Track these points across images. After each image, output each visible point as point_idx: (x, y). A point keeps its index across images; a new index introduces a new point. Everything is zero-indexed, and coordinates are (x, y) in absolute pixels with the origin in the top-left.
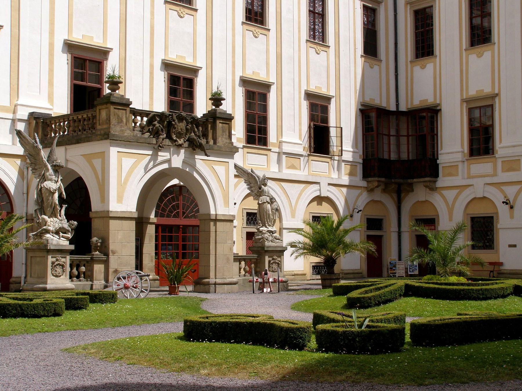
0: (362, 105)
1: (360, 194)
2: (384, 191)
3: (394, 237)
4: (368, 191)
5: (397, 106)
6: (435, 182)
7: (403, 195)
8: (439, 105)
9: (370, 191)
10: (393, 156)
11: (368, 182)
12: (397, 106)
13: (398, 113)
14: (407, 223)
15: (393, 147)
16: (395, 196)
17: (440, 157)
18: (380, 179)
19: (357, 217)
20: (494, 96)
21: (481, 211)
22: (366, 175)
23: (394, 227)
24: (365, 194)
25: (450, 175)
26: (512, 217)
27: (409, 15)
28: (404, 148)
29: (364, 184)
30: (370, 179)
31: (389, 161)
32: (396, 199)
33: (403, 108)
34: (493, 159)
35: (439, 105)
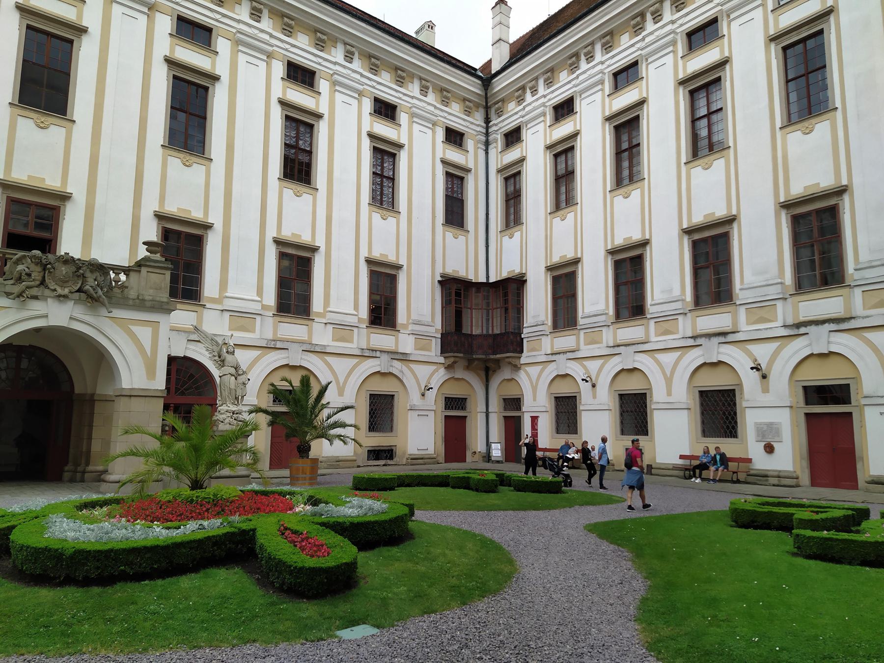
2: (468, 368)
3: (481, 419)
7: (490, 373)
9: (449, 367)
10: (476, 331)
13: (487, 285)
14: (495, 405)
16: (483, 374)
17: (525, 331)
18: (456, 354)
19: (431, 395)
20: (576, 262)
21: (564, 389)
22: (443, 351)
23: (482, 407)
24: (442, 371)
26: (594, 397)
29: (442, 360)
30: (447, 355)
31: (471, 335)
32: (484, 377)
33: (492, 280)
34: (575, 332)
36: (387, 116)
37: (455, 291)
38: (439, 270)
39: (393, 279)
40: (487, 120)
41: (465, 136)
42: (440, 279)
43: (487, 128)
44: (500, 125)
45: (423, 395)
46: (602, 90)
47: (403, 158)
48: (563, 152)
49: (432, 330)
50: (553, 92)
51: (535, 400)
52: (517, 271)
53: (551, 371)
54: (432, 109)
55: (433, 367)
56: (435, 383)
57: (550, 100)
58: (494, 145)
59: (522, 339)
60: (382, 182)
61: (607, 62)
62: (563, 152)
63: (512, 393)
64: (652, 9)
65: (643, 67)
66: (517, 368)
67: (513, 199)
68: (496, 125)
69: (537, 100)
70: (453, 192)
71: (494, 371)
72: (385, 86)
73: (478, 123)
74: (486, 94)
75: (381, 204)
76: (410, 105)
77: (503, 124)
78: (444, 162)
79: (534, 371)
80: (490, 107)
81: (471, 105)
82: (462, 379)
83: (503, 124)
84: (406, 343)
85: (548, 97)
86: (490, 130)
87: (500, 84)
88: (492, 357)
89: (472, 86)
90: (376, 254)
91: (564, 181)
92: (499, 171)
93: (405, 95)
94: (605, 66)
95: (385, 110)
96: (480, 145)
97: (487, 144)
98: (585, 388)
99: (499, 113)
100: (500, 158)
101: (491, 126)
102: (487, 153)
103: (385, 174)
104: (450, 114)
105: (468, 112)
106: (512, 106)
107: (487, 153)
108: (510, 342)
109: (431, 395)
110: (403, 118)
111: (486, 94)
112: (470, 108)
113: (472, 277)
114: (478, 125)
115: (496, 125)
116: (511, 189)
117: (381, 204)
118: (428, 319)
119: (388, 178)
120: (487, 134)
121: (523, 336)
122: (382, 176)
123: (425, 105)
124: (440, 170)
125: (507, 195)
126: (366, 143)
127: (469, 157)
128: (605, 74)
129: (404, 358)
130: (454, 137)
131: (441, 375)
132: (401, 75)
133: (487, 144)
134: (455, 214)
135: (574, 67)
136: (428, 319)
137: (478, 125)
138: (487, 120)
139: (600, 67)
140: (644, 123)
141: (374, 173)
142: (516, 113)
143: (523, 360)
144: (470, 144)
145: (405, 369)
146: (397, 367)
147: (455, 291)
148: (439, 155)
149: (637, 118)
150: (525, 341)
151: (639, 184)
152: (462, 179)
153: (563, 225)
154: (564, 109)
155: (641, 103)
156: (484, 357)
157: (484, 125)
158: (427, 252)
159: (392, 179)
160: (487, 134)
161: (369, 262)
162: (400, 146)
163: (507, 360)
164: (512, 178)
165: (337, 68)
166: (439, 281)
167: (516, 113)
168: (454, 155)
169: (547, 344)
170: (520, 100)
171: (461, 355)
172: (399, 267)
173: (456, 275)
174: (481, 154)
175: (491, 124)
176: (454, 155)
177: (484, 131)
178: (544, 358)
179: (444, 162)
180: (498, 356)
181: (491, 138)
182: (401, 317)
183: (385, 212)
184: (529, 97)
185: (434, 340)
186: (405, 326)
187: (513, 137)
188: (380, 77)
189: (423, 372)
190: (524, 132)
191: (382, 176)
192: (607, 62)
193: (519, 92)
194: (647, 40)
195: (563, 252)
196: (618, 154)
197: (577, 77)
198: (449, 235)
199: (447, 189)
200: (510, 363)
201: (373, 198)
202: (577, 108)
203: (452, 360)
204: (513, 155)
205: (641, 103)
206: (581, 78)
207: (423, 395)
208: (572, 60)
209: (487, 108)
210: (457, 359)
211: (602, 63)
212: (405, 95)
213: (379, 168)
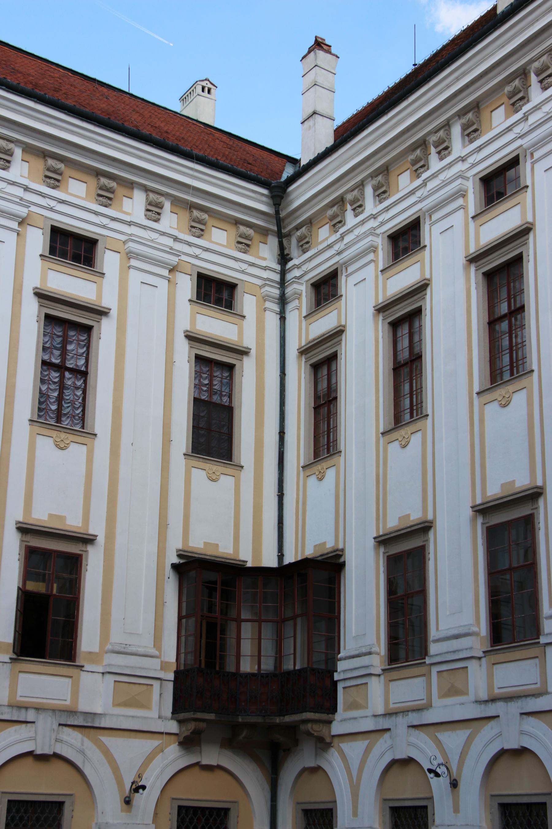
0: (180, 556)
1: (160, 750)
4: (181, 744)
5: (281, 556)
6: (330, 722)
8: (343, 550)
9: (188, 743)
10: (247, 666)
11: (180, 722)
12: (281, 556)
15: (247, 647)
17: (341, 666)
18: (199, 715)
19: (146, 801)
21: (406, 791)
22: (180, 705)
25: (353, 706)
26: (456, 810)
27: (303, 375)
28: (288, 647)
29: (173, 727)
30: (182, 716)
31: (237, 675)
35: (343, 550)
36: (76, 258)
37: (209, 585)
38: (175, 544)
39: (73, 565)
40: (284, 258)
41: (239, 290)
42: (176, 560)
43: (283, 273)
44: (304, 268)
45: (128, 802)
46: (463, 207)
47: (106, 333)
48: (404, 318)
49: (156, 664)
50: (387, 209)
51: (355, 814)
52: (330, 545)
53: (383, 752)
54: (169, 242)
55: (153, 743)
56: (155, 779)
57: (382, 224)
58: (296, 303)
59: (335, 683)
60: (62, 377)
61: (467, 160)
62: (404, 318)
63: (315, 797)
64: (536, 65)
65: (526, 167)
66: (323, 744)
67: (325, 405)
68: (298, 267)
69: (363, 222)
70: (211, 391)
71: (288, 751)
72: (76, 205)
73: (264, 264)
74: (277, 212)
75: (59, 420)
76: (123, 238)
77: (308, 266)
78: (192, 338)
79: (354, 750)
80: (289, 235)
81: (250, 232)
82: (219, 767)
83: (308, 266)
84: (94, 692)
85: (380, 219)
86: (289, 276)
87: (302, 193)
88: (278, 720)
89: (251, 197)
90: (41, 516)
91: (406, 370)
92: (303, 352)
93: (114, 219)
94: (466, 165)
95: (73, 248)
96: (268, 304)
97: (283, 301)
98: (439, 786)
99: (304, 245)
100: (303, 329)
101: (290, 270)
102: (283, 319)
103: (70, 364)
104: (207, 250)
105: (244, 244)
106: (324, 234)
107: (283, 319)
108: (313, 690)
109: (146, 801)
110: (109, 261)
111: (277, 212)
112: (247, 237)
113: (247, 556)
114: (265, 268)
115: (298, 267)
116: (323, 385)
117: (59, 420)
118: (146, 643)
119: (75, 371)
120: (282, 283)
121: (336, 677)
122: (61, 368)
123: (154, 236)
124: (183, 354)
125: (317, 397)
126: (31, 310)
127: (250, 326)
128: (467, 179)
129: (90, 726)
130: (215, 292)
131: (172, 758)
132: (110, 184)
133: (283, 301)
134: (213, 432)
135: (419, 166)
136: (146, 643)
137: (265, 268)
139: (460, 167)
140: (529, 268)
141: (44, 363)
142: (330, 246)
143: (337, 728)
144: (247, 303)
145: (88, 745)
146: (72, 744)
147: (209, 585)
148: (183, 323)
149: (519, 260)
150: (340, 686)
151: (524, 382)
152: (230, 368)
153: (404, 458)
154: (406, 240)
155: (524, 232)
156: (259, 720)
157: (278, 267)
159: (83, 374)
160: (282, 283)
161: (24, 530)
162: (101, 313)
163: (303, 727)
164: (323, 361)
166: (175, 567)
167: (330, 246)
168: (214, 325)
169: (378, 695)
170: (337, 223)
171: (211, 716)
172: (88, 540)
173: (210, 553)
174: (272, 321)
175: (290, 264)
176: (214, 325)
177: (277, 277)
178: (368, 725)
179: (192, 338)
180: (288, 719)
181: (289, 291)
182: (88, 638)
183: (63, 436)
184: (351, 220)
185: (156, 685)
186: (94, 657)
187: (326, 289)
189: (130, 753)
190: (342, 280)
192: (467, 160)
193: (338, 206)
194: (533, 119)
195: (404, 510)
196: (493, 322)
197: (424, 184)
198: (199, 476)
199: (198, 386)
200: (309, 734)
201: (40, 410)
202: (426, 239)
203: (192, 726)
204: (324, 324)
205: (524, 232)
206: (431, 185)
207: (128, 802)
208: (418, 151)
209: (281, 236)
210: (203, 725)
211: (463, 159)
212: (114, 219)
213: (57, 353)
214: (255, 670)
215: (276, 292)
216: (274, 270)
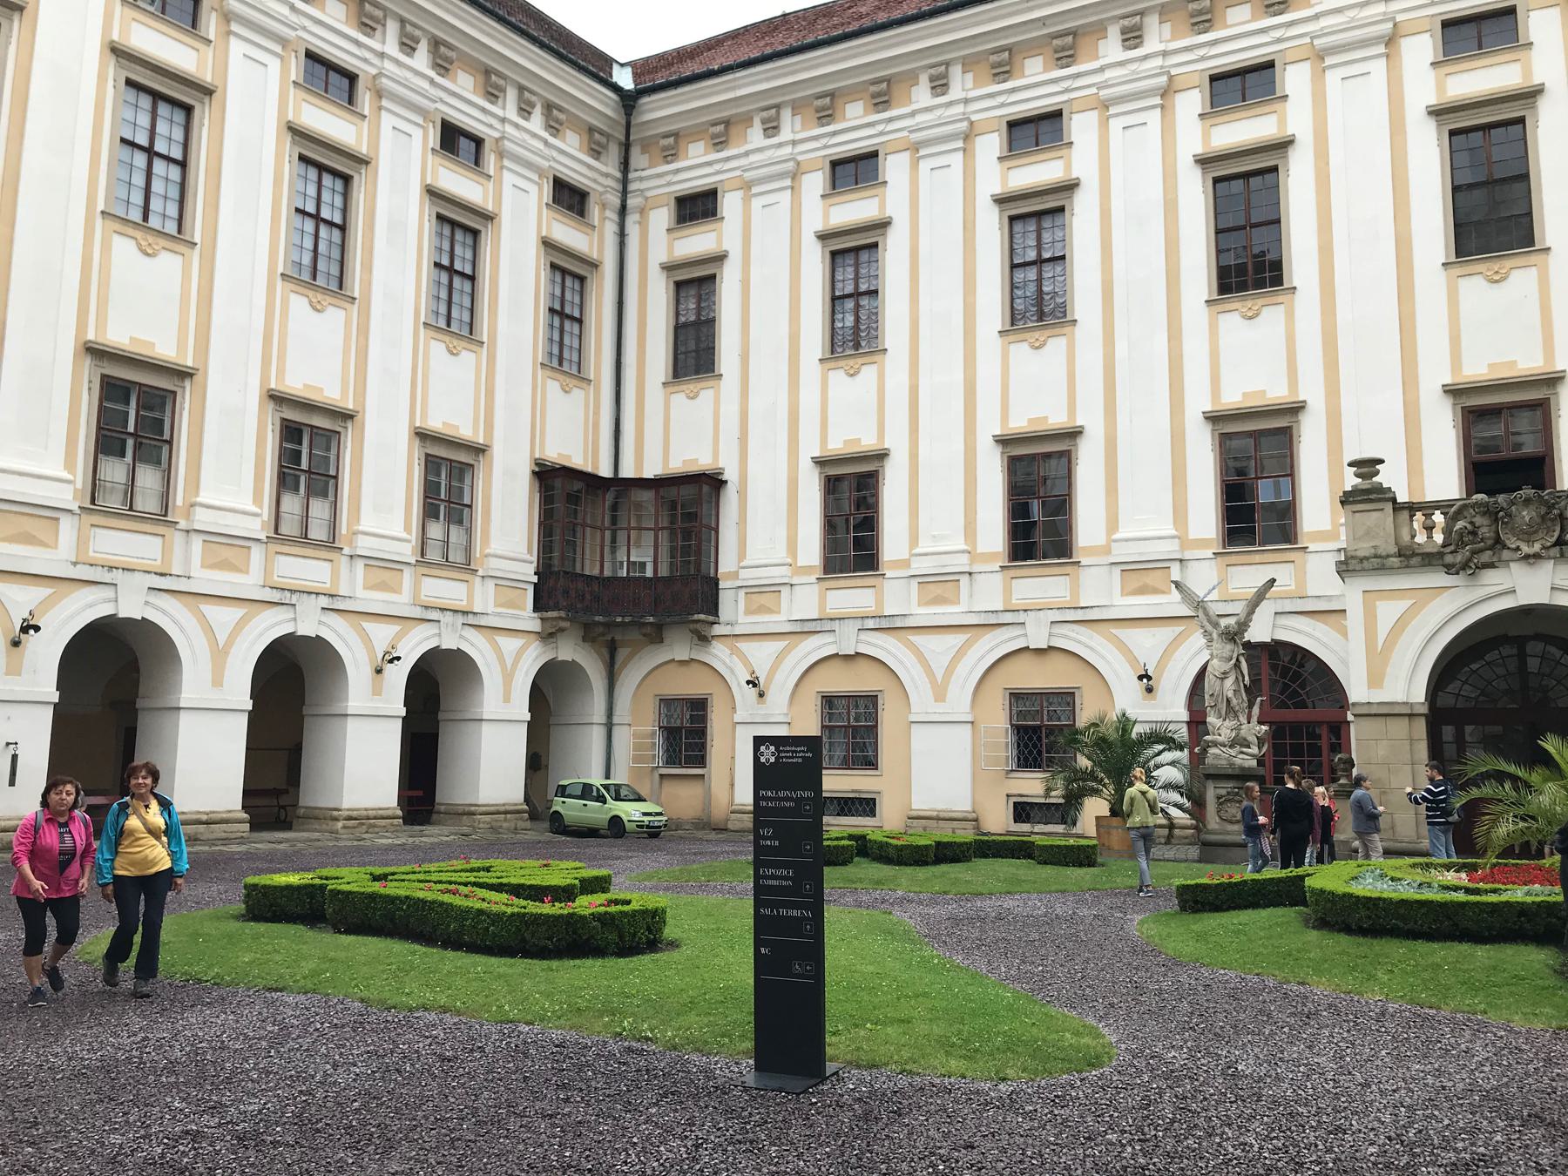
40: (625, 166)
114: (607, 175)
115: (641, 179)
122: (450, 270)
130: (570, 198)
137: (607, 175)
138: (625, 166)
144: (594, 212)
157: (619, 175)
158: (528, 420)
165: (388, 65)
168: (568, 234)
177: (620, 187)
181: (631, 202)
188: (454, 81)
191: (450, 270)
214: (596, 572)
215: (617, 202)
216: (613, 177)
